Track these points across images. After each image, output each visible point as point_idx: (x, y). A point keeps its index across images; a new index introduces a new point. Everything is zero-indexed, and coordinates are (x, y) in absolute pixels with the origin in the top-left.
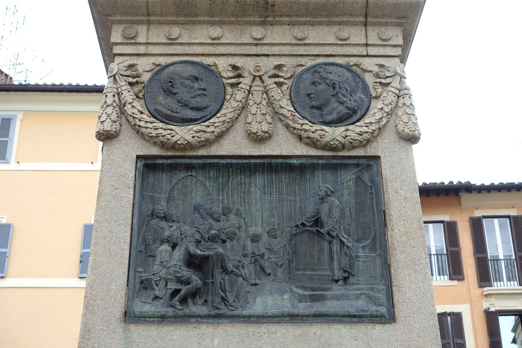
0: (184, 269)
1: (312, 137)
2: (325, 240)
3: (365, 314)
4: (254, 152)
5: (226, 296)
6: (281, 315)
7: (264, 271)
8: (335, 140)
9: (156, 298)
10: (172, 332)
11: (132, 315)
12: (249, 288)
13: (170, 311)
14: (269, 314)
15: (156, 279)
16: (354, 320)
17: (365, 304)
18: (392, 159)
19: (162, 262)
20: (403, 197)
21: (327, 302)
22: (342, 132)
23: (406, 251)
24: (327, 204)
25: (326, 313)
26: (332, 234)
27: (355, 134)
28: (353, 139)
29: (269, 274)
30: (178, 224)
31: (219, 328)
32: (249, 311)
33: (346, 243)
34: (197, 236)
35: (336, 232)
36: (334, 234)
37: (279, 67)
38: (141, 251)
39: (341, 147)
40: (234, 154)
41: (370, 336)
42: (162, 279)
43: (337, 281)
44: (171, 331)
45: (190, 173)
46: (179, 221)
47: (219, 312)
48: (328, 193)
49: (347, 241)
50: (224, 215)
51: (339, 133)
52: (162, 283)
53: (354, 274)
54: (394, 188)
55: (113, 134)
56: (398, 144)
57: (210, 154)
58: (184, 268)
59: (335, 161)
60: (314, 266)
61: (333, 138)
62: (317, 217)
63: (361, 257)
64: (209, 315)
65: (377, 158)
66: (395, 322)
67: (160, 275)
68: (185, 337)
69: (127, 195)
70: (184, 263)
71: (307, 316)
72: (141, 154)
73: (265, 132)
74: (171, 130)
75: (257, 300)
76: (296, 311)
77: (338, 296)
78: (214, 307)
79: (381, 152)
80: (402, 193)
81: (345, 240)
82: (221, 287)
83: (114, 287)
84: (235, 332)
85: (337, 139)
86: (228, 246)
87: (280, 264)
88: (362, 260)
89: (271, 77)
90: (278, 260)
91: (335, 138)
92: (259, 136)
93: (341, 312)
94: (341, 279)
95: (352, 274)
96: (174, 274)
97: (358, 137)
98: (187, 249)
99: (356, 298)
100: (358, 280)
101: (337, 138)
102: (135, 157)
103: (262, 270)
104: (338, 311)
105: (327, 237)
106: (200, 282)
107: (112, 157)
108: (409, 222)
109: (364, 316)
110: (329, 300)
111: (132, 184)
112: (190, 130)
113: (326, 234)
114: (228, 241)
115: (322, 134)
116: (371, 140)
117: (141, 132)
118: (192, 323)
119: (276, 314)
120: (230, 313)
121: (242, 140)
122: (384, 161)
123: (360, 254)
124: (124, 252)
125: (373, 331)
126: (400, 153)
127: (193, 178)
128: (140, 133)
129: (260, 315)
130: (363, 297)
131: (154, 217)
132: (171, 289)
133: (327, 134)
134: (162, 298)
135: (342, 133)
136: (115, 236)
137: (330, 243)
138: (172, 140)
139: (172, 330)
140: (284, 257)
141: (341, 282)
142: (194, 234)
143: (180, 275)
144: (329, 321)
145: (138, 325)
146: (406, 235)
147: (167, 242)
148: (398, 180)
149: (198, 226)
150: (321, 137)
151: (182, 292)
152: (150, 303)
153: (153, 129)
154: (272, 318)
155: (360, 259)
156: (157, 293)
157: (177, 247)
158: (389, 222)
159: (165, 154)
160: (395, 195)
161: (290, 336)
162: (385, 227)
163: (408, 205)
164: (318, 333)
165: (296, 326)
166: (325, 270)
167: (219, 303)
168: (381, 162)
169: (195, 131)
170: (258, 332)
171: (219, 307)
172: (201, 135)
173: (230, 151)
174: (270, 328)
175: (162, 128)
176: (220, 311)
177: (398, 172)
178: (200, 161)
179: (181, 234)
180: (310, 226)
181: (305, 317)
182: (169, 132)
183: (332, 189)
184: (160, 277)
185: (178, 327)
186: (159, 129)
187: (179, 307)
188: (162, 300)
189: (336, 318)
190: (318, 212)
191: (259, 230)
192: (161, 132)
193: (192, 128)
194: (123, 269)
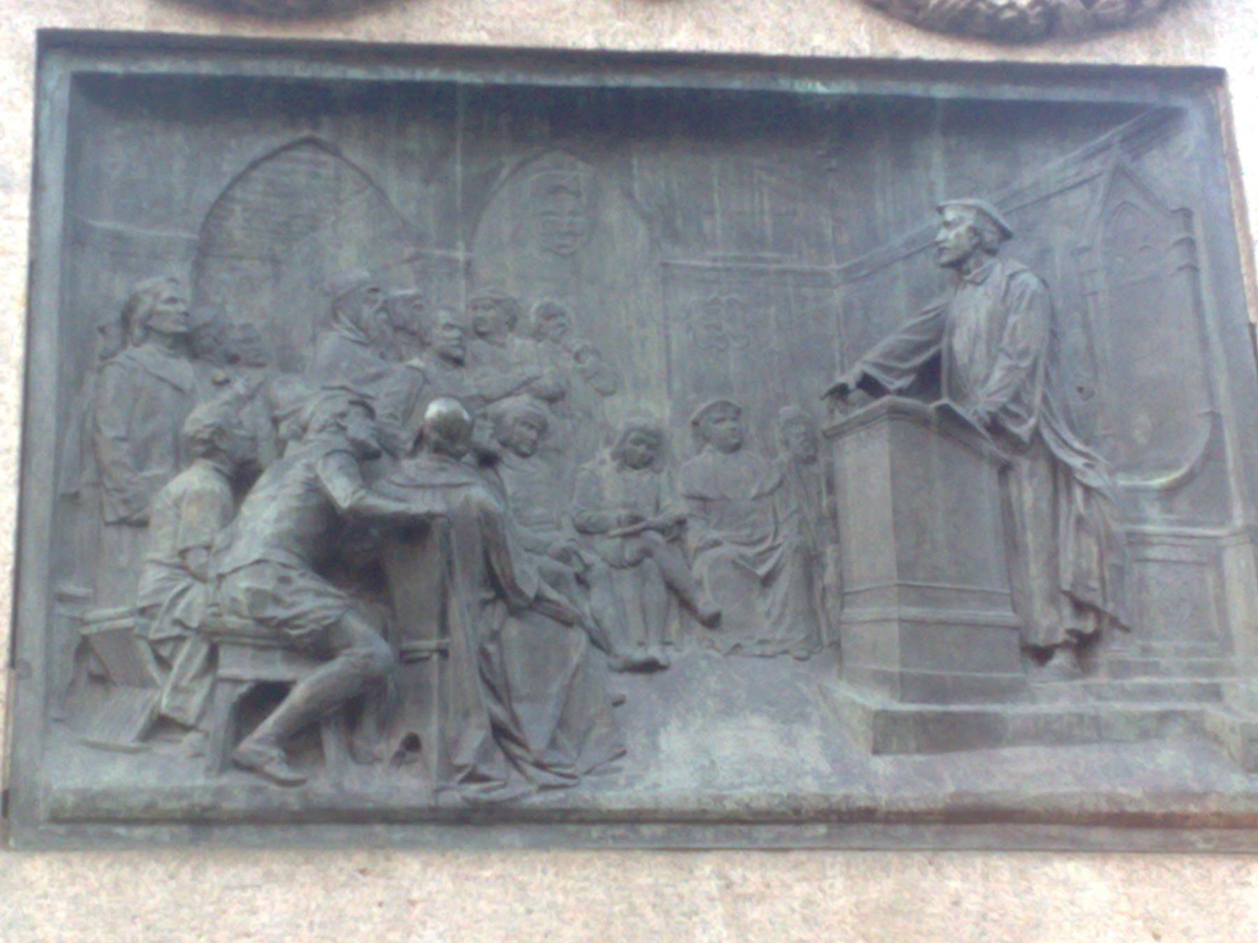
0: (301, 583)
2: (980, 455)
3: (1193, 808)
5: (515, 719)
6: (791, 813)
7: (686, 604)
9: (161, 725)
10: (249, 893)
11: (42, 811)
12: (622, 685)
14: (729, 806)
15: (157, 631)
19: (183, 553)
21: (1007, 752)
24: (981, 289)
25: (1006, 802)
29: (713, 622)
30: (256, 376)
32: (629, 791)
33: (1083, 474)
34: (359, 428)
35: (1032, 422)
36: (1023, 431)
38: (76, 495)
42: (186, 633)
43: (1042, 655)
44: (243, 888)
45: (305, 133)
46: (260, 360)
47: (484, 797)
50: (482, 335)
52: (190, 656)
53: (1124, 621)
58: (306, 581)
59: (1009, 92)
63: (1155, 540)
64: (434, 810)
67: (178, 613)
68: (318, 918)
70: (298, 556)
71: (915, 818)
75: (663, 742)
76: (860, 795)
77: (1056, 726)
78: (459, 769)
81: (1077, 462)
82: (488, 676)
84: (565, 891)
86: (506, 481)
87: (762, 570)
90: (751, 552)
94: (1065, 645)
95: (1114, 622)
96: (252, 606)
98: (314, 487)
99: (1144, 735)
100: (1146, 650)
102: (31, 39)
103: (674, 602)
104: (1065, 795)
105: (989, 446)
106: (383, 649)
110: (1011, 743)
111: (22, 168)
113: (983, 431)
114: (510, 458)
119: (762, 804)
120: (537, 800)
123: (1150, 528)
125: (1235, 892)
127: (324, 157)
130: (1177, 729)
131: (137, 332)
132: (237, 681)
134: (186, 728)
137: (1004, 470)
140: (780, 540)
141: (1060, 659)
142: (343, 415)
143: (282, 613)
145: (75, 857)
147: (206, 455)
149: (355, 381)
151: (297, 696)
152: (134, 751)
154: (744, 828)
155: (1153, 553)
156: (165, 702)
157: (263, 480)
164: (972, 903)
166: (988, 598)
167: (484, 755)
171: (484, 770)
173: (507, 25)
174: (736, 874)
176: (488, 791)
178: (357, 73)
179: (276, 421)
180: (900, 392)
183: (1003, 221)
184: (178, 622)
185: (276, 868)
187: (284, 772)
188: (192, 737)
189: (1054, 830)
190: (940, 327)
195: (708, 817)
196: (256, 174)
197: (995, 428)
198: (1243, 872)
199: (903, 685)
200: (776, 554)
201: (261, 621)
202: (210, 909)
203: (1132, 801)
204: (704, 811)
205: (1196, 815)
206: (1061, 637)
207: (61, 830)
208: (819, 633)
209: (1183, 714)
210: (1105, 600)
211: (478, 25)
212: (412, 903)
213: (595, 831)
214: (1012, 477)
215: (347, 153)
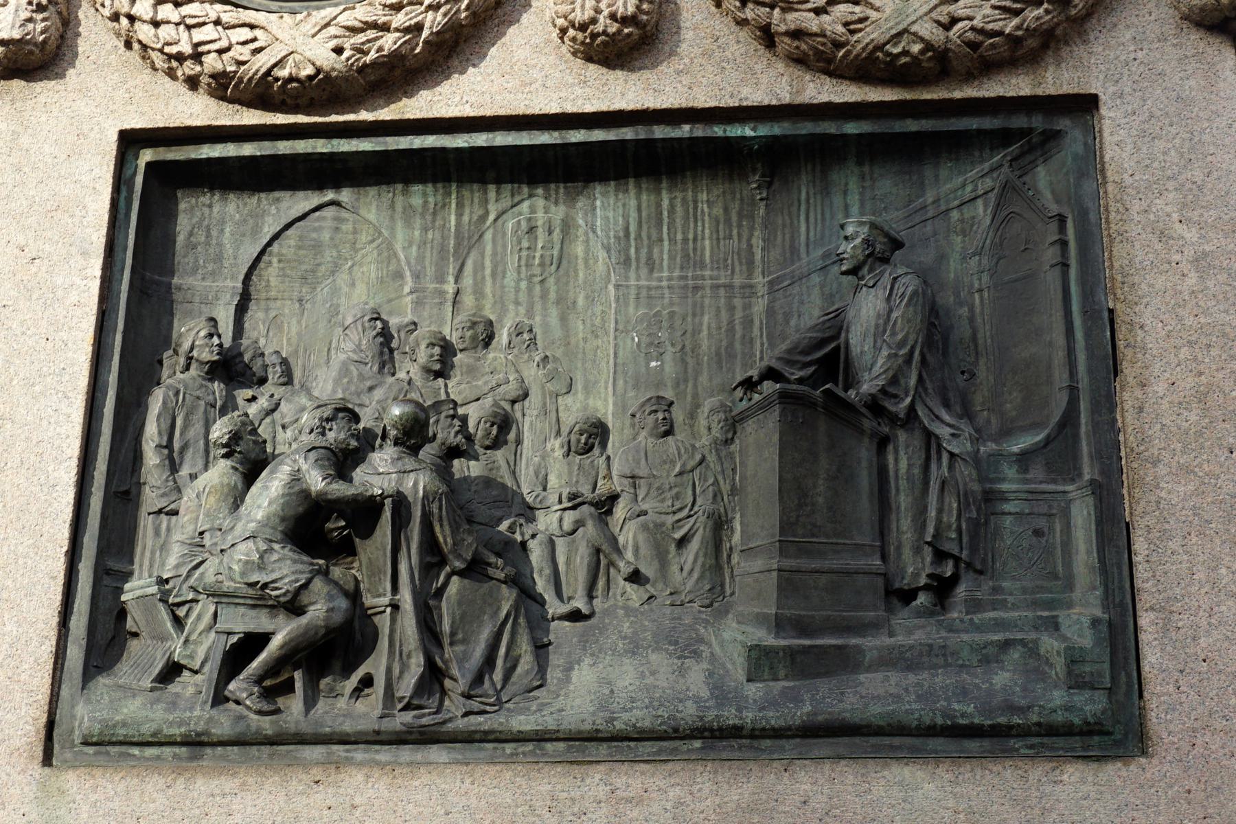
1: (815, 29)
2: (862, 432)
3: (1017, 720)
4: (580, 102)
6: (670, 731)
8: (906, 35)
13: (223, 723)
14: (619, 725)
16: (973, 745)
17: (1020, 682)
18: (1149, 102)
20: (1189, 253)
21: (862, 677)
22: (935, 7)
23: (1200, 466)
25: (856, 718)
26: (893, 409)
27: (988, 11)
28: (981, 31)
31: (417, 783)
35: (909, 400)
39: (931, 65)
40: (502, 112)
41: (1037, 811)
48: (878, 247)
49: (953, 435)
51: (925, 8)
54: (1152, 217)
55: (31, 52)
56: (1175, 45)
57: (407, 116)
59: (912, 126)
60: (813, 536)
61: (900, 27)
62: (833, 345)
63: (1012, 496)
64: (378, 733)
65: (1086, 104)
66: (1144, 753)
69: (78, 281)
71: (777, 734)
72: (138, 126)
73: (625, 21)
74: (252, 27)
75: (575, 675)
76: (730, 716)
77: (908, 655)
79: (1101, 77)
80: (1188, 235)
81: (943, 432)
83: (8, 628)
85: (915, 34)
88: (1013, 510)
91: (905, 31)
92: (598, 35)
93: (916, 716)
94: (926, 588)
96: (243, 574)
97: (1001, 23)
99: (985, 661)
100: (996, 590)
101: (914, 28)
102: (114, 137)
105: (868, 424)
107: (25, 140)
108: (1215, 352)
109: (1014, 732)
110: (869, 670)
112: (327, 25)
113: (864, 410)
115: (855, 17)
116: (1059, 32)
117: (140, 42)
118: (306, 765)
119: (647, 724)
121: (535, 55)
122: (1110, 116)
123: (1005, 487)
124: (55, 495)
125: (1048, 789)
126: (1181, 79)
127: (344, 214)
128: (136, 46)
129: (580, 732)
130: (1015, 654)
133: (874, 15)
135: (939, 9)
136: (23, 437)
138: (254, 63)
139: (227, 791)
140: (696, 509)
141: (922, 599)
143: (264, 578)
144: (866, 752)
145: (98, 772)
146: (1200, 402)
148: (1171, 185)
150: (852, 27)
153: (182, 27)
154: (632, 744)
155: (1008, 507)
158: (1129, 353)
159: (229, 123)
160: (1158, 246)
161: (702, 812)
162: (1116, 375)
163: (1210, 284)
165: (727, 775)
168: (1101, 118)
169: (348, 28)
170: (573, 800)
172: (369, 41)
174: (620, 782)
175: (217, 22)
177: (1173, 153)
180: (800, 381)
181: (770, 737)
182: (245, 34)
185: (250, 780)
186: (204, 24)
189: (897, 741)
190: (835, 326)
191: (605, 407)
192: (215, 36)
193: (335, 18)
194: (50, 561)
195: (600, 735)
196: (289, 232)
197: (875, 406)
198: (1058, 772)
199: (780, 624)
200: (692, 520)
201: (252, 585)
202: (197, 812)
203: (963, 715)
204: (597, 731)
205: (1019, 725)
206: (923, 581)
207: (91, 750)
208: (722, 585)
209: (1022, 642)
210: (961, 549)
211: (464, 100)
212: (355, 807)
213: (509, 748)
214: (890, 448)
215: (363, 212)
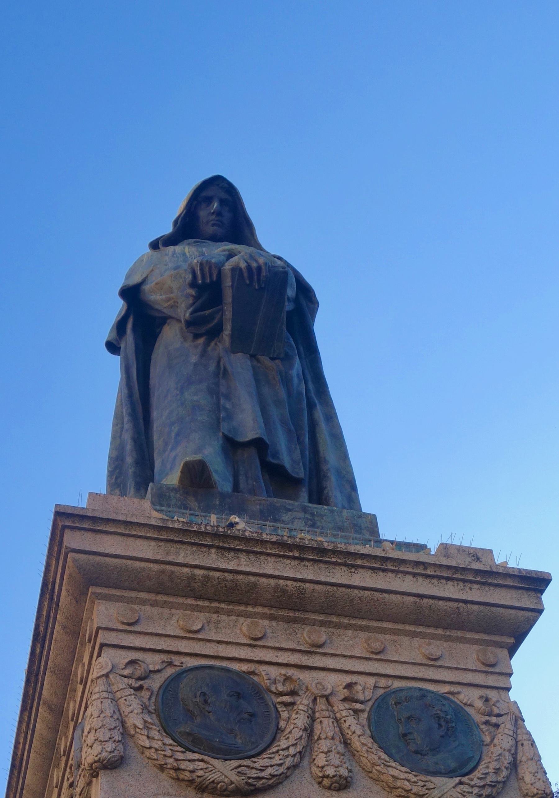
37: (349, 686)
89: (345, 700)
